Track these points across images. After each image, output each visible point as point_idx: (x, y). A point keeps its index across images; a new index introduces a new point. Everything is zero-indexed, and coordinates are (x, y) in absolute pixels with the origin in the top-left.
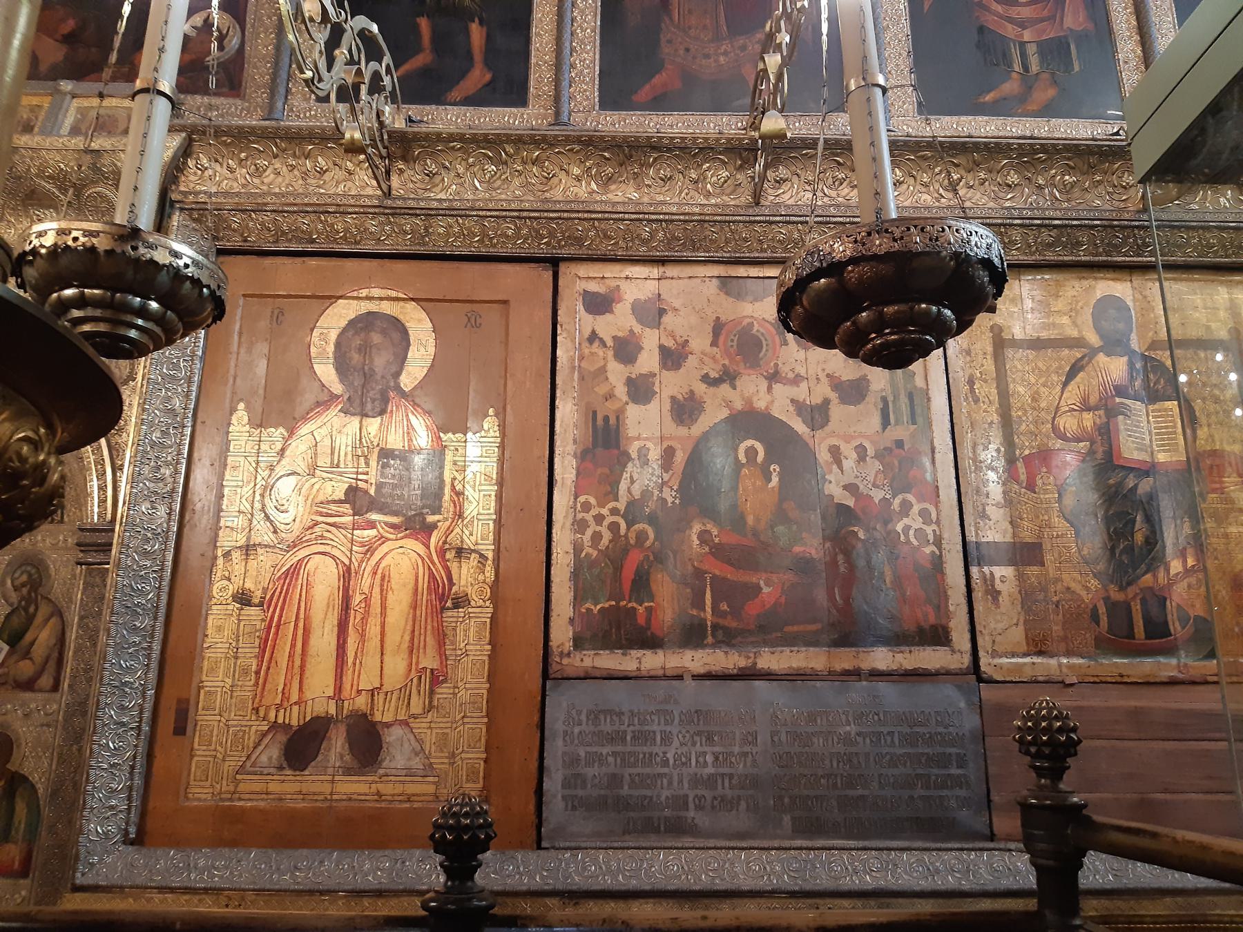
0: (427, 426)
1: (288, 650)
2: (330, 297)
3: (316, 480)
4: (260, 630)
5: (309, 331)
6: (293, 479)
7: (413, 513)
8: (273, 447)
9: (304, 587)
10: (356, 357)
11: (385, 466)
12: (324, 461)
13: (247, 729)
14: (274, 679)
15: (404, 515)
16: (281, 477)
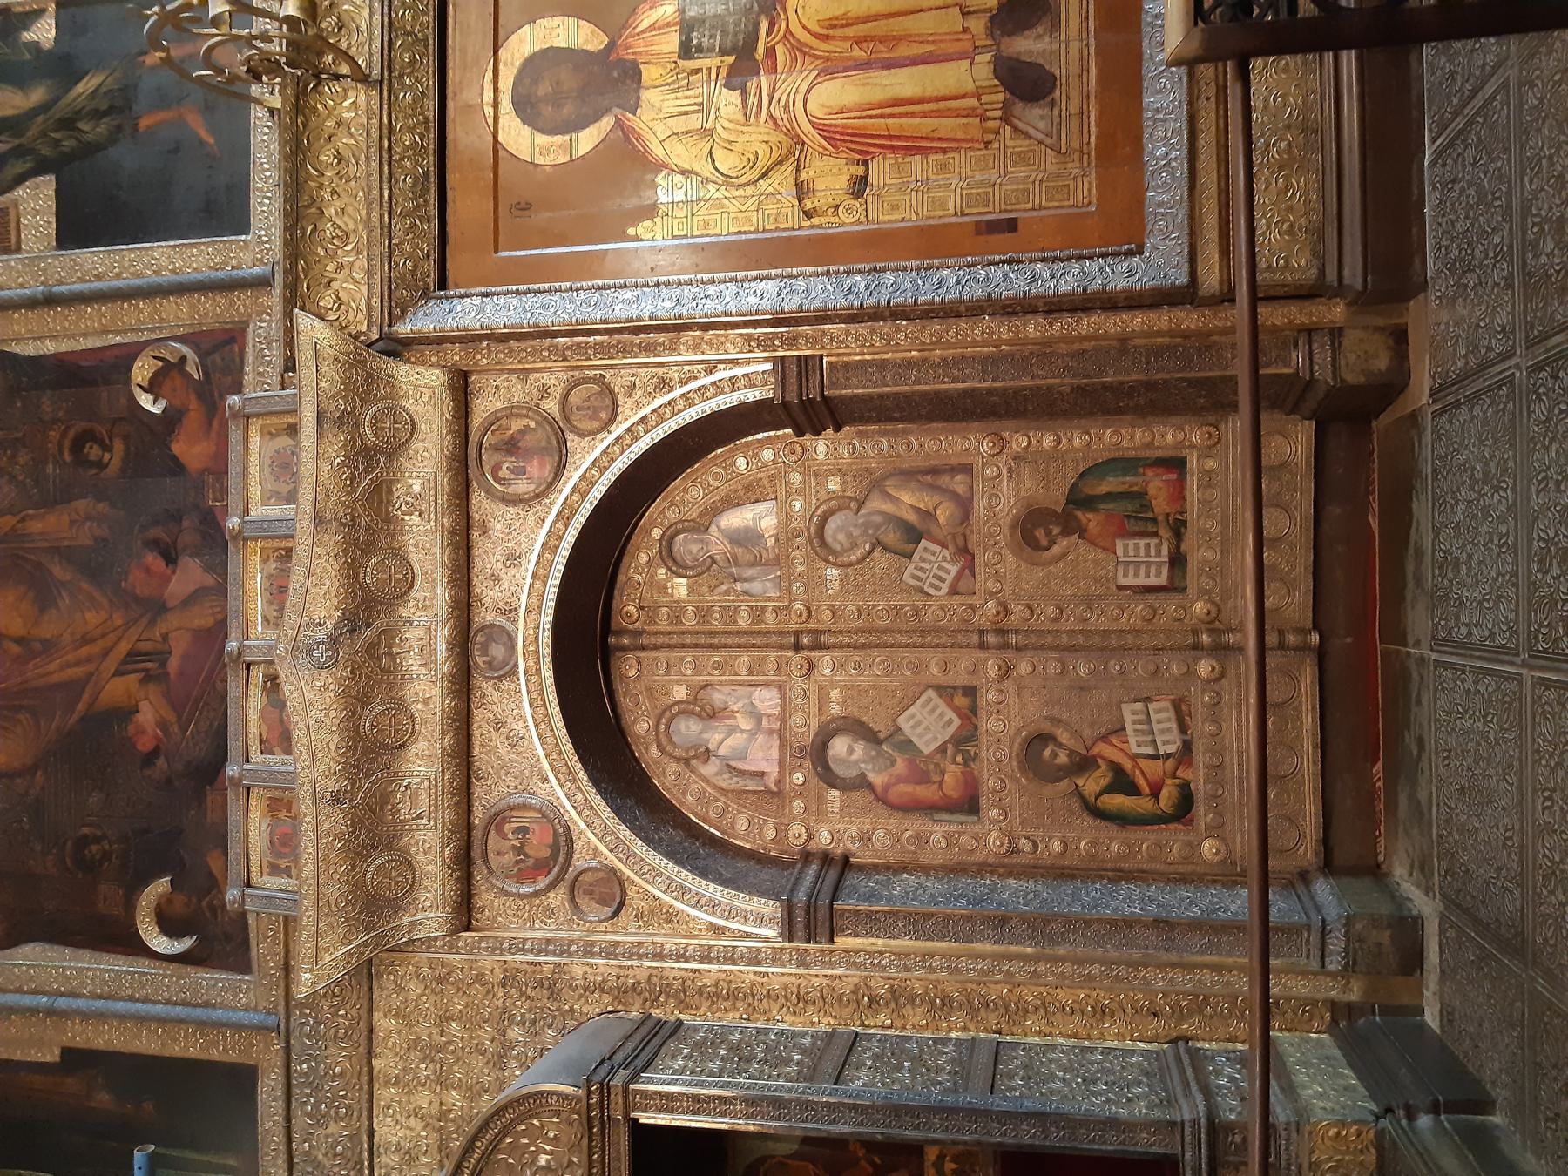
0: (651, 8)
1: (917, 121)
2: (496, 151)
3: (718, 126)
4: (896, 159)
5: (539, 169)
6: (718, 153)
7: (755, 5)
8: (679, 185)
9: (845, 115)
10: (568, 110)
11: (700, 49)
12: (695, 122)
13: (1009, 151)
14: (952, 129)
15: (758, 15)
16: (716, 169)
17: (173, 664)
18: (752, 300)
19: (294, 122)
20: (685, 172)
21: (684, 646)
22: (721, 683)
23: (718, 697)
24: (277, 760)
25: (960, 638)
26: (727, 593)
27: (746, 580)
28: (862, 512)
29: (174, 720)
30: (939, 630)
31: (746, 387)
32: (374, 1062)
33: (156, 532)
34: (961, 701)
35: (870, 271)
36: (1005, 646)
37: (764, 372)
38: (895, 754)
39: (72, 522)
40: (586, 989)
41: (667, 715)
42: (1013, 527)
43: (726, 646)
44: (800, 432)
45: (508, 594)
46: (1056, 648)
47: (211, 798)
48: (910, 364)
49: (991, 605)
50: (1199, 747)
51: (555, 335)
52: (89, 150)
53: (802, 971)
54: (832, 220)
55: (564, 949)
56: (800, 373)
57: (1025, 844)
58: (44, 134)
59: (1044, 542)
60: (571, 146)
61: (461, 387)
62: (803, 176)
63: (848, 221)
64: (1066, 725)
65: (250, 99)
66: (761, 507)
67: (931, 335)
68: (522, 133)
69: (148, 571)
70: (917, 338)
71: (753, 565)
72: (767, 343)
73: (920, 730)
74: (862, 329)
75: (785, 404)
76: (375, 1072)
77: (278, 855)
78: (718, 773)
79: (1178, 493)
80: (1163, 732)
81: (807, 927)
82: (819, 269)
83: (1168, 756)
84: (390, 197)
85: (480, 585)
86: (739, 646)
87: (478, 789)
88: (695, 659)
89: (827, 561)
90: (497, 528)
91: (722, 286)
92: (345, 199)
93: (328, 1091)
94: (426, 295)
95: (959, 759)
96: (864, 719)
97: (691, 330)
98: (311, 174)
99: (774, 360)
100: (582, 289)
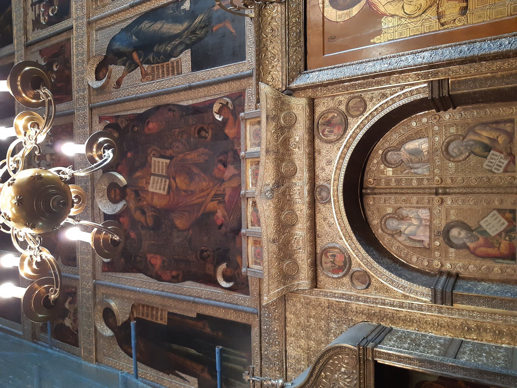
8: (390, 21)
16: (405, 13)
17: (227, 198)
18: (420, 60)
19: (258, 20)
20: (392, 16)
21: (391, 193)
23: (404, 212)
24: (256, 228)
25: (508, 190)
26: (408, 173)
27: (415, 168)
28: (465, 140)
29: (227, 215)
30: (498, 187)
31: (417, 94)
32: (287, 328)
33: (221, 158)
34: (508, 215)
35: (469, 43)
37: (424, 87)
38: (479, 236)
39: (198, 155)
40: (357, 312)
41: (385, 218)
43: (407, 193)
44: (438, 111)
45: (328, 175)
47: (237, 239)
48: (487, 79)
51: (344, 82)
52: (200, 39)
53: (440, 315)
54: (453, 25)
55: (349, 297)
56: (439, 86)
58: (187, 37)
60: (350, 13)
61: (312, 104)
62: (440, 10)
63: (459, 25)
65: (244, 15)
66: (422, 140)
67: (497, 66)
68: (333, 11)
69: (219, 169)
70: (490, 68)
71: (418, 162)
72: (425, 76)
73: (490, 226)
74: (466, 67)
75: (433, 99)
76: (287, 332)
77: (257, 258)
81: (442, 299)
82: (448, 45)
84: (289, 41)
85: (318, 172)
86: (413, 193)
87: (318, 241)
89: (449, 160)
90: (324, 152)
91: (407, 56)
92: (274, 43)
93: (272, 336)
94: (300, 73)
95: (507, 238)
96: (466, 222)
97: (395, 74)
98: (264, 37)
99: (428, 82)
100: (354, 64)
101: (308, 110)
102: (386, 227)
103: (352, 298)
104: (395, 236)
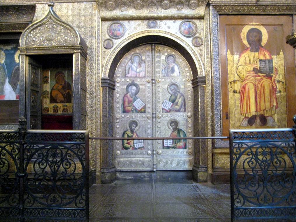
2: (244, 25)
21: (152, 58)
22: (145, 65)
23: (143, 65)
30: (156, 106)
34: (143, 110)
36: (153, 118)
38: (133, 98)
42: (175, 119)
43: (152, 66)
44: (192, 81)
46: (153, 127)
49: (160, 116)
50: (136, 151)
53: (96, 82)
57: (118, 121)
59: (172, 125)
61: (201, 18)
62: (237, 82)
64: (139, 129)
71: (168, 72)
73: (138, 102)
78: (129, 65)
79: (180, 148)
80: (138, 145)
83: (134, 146)
86: (152, 69)
88: (150, 61)
94: (218, 12)
95: (132, 110)
96: (139, 92)
101: (198, 16)
102: (135, 56)
103: (98, 40)
104: (131, 61)
